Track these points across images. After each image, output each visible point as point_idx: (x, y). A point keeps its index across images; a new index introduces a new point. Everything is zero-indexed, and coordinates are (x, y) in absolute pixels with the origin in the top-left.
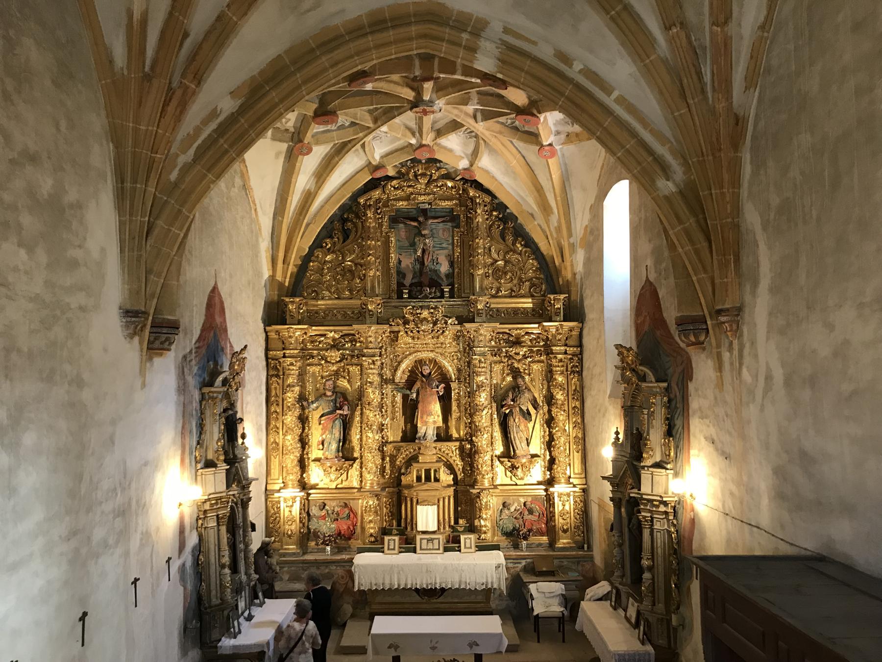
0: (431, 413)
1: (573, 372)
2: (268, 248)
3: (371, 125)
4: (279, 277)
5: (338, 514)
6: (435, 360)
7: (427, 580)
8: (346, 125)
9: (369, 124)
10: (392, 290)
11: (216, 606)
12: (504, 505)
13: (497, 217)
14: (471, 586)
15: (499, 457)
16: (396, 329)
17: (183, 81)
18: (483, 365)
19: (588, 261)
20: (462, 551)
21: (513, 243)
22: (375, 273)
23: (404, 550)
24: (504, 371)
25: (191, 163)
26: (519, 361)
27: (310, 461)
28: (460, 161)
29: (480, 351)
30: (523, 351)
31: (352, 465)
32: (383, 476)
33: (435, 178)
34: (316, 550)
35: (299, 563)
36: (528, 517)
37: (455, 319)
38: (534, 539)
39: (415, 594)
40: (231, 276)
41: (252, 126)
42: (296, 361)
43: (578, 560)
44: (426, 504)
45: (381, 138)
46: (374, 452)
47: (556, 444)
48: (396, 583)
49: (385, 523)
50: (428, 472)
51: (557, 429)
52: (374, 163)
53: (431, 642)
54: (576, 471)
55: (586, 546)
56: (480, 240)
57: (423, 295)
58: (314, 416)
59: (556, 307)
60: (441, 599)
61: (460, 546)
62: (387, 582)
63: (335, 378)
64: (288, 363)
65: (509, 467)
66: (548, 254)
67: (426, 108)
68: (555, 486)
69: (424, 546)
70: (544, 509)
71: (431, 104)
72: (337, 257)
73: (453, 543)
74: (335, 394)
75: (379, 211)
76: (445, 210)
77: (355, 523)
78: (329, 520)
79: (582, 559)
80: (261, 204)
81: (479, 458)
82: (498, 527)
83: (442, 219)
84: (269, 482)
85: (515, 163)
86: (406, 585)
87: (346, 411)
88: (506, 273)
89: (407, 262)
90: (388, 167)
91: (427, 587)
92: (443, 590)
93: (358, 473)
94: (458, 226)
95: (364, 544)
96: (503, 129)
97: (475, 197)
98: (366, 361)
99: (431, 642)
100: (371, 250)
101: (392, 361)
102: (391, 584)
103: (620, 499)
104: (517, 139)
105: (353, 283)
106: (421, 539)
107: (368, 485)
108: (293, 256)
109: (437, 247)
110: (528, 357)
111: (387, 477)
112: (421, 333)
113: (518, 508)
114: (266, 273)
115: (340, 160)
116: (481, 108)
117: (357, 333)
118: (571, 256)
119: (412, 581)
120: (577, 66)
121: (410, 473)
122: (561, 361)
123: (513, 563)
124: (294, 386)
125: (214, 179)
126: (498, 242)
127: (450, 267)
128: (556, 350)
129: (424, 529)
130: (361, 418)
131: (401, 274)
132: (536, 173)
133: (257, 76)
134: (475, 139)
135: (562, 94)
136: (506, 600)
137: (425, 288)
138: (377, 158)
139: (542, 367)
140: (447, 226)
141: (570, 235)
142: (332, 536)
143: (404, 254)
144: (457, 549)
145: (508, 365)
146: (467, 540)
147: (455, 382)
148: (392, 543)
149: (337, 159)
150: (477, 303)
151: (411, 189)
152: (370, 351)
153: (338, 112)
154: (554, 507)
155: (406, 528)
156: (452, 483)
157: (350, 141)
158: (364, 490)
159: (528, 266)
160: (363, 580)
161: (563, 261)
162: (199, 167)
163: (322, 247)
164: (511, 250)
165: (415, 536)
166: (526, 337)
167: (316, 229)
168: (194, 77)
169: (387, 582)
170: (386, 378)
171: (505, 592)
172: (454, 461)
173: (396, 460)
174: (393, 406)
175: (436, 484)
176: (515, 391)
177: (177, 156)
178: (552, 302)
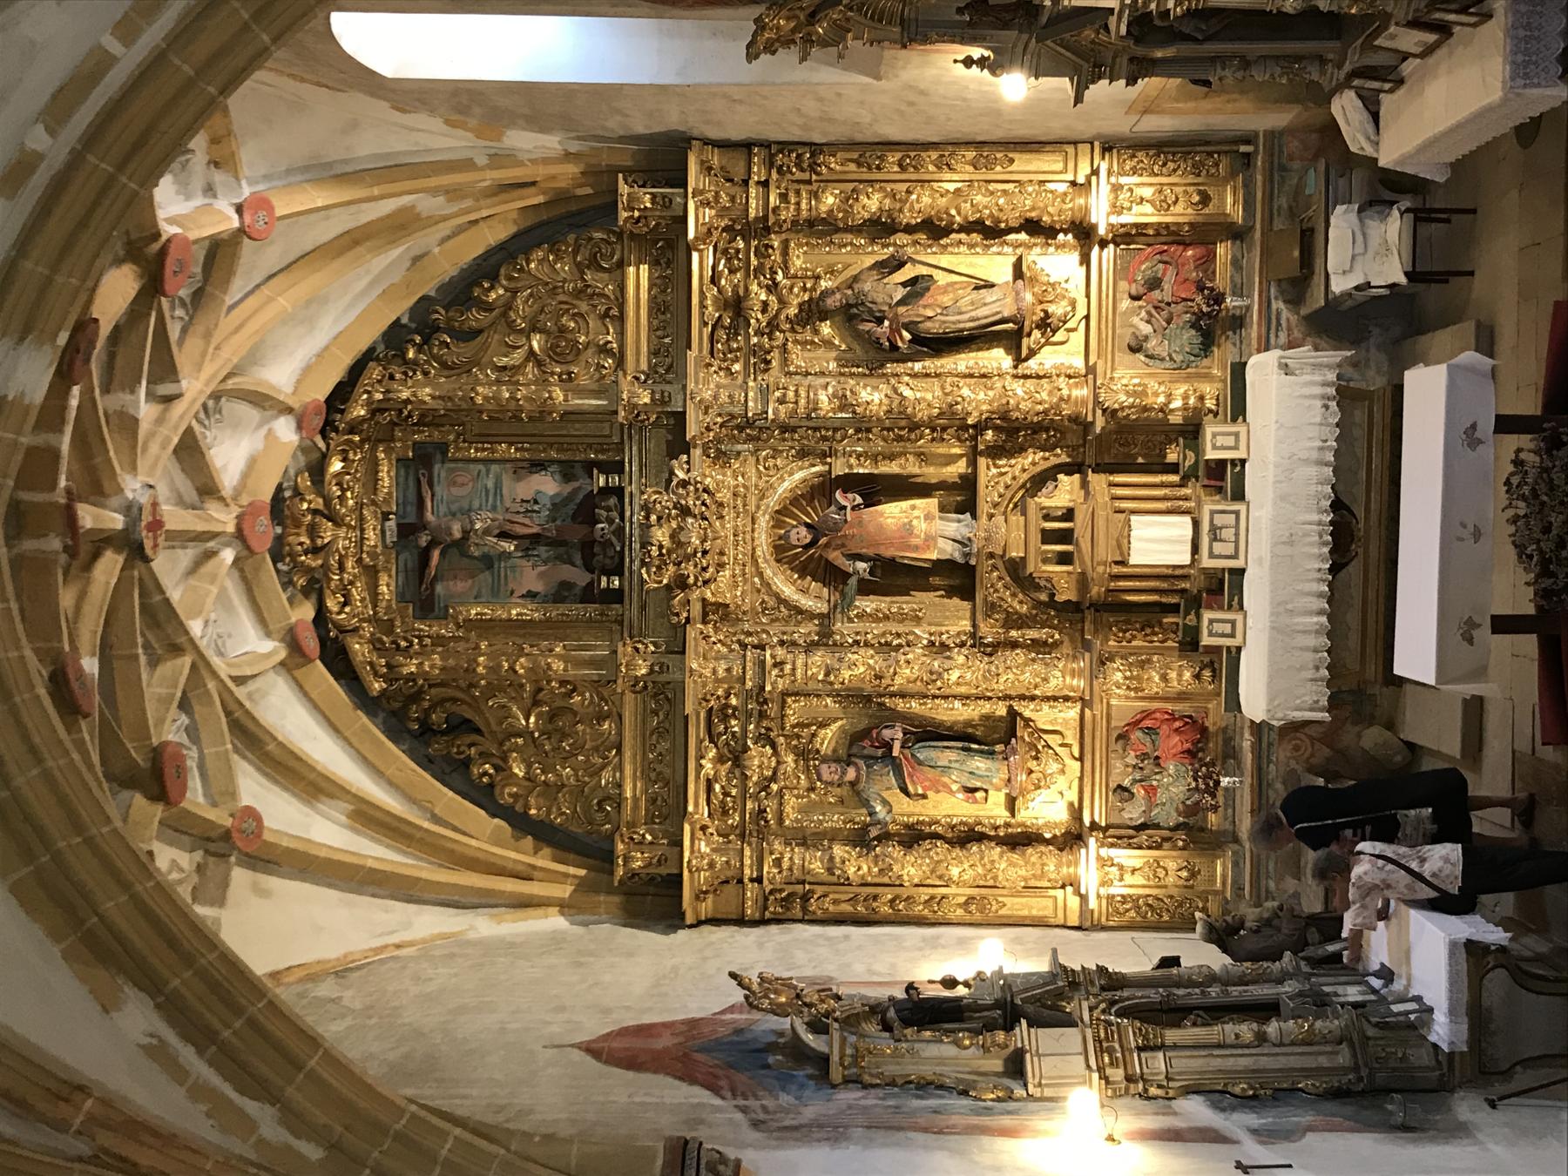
0: (905, 524)
1: (813, 168)
2: (492, 916)
3: (187, 661)
4: (564, 891)
5: (1144, 756)
6: (777, 512)
7: (1311, 544)
8: (187, 721)
9: (183, 666)
10: (601, 615)
11: (1354, 1055)
12: (1134, 349)
13: (420, 350)
15: (1019, 360)
16: (696, 609)
17: (73, 1129)
18: (791, 394)
19: (537, 122)
20: (1244, 456)
21: (486, 310)
22: (559, 657)
23: (1236, 598)
24: (805, 343)
25: (279, 1110)
26: (783, 303)
27: (1013, 821)
29: (756, 401)
30: (759, 294)
31: (1027, 721)
32: (1056, 645)
33: (320, 501)
34: (1230, 811)
37: (674, 462)
38: (1222, 278)
39: (1342, 574)
40: (561, 1009)
41: (188, 960)
42: (771, 853)
43: (1277, 170)
44: (1126, 541)
45: (220, 637)
46: (997, 668)
47: (991, 215)
48: (1315, 619)
49: (1170, 643)
50: (1048, 537)
51: (953, 212)
52: (283, 654)
53: (1462, 540)
54: (1059, 166)
55: (1243, 149)
56: (477, 394)
57: (614, 540)
58: (905, 809)
59: (648, 205)
60: (1360, 512)
61: (1233, 462)
62: (1312, 641)
63: (814, 759)
64: (776, 871)
65: (1043, 334)
66: (515, 222)
67: (143, 524)
68: (1093, 220)
69: (1228, 549)
70: (1149, 250)
71: (135, 510)
72: (516, 748)
73: (1222, 478)
74: (853, 759)
75: (403, 644)
76: (401, 480)
77: (1166, 716)
78: (1158, 777)
79: (1276, 161)
81: (1018, 408)
82: (1188, 367)
83: (425, 487)
84: (1061, 922)
85: (284, 300)
86: (1320, 595)
87: (896, 734)
88: (563, 330)
89: (531, 576)
90: (293, 620)
91: (1325, 544)
92: (1337, 505)
93: (1045, 707)
94: (443, 448)
95: (1219, 694)
96: (199, 328)
97: (369, 402)
98: (776, 682)
99: (1462, 540)
100: (500, 666)
101: (777, 620)
102: (1317, 632)
103: (1131, 60)
104: (225, 293)
105: (581, 711)
106: (1212, 555)
107: (1075, 682)
108: (513, 855)
109: (495, 501)
110: (773, 280)
111: (1057, 636)
112: (707, 546)
113: (1143, 314)
114: (555, 922)
115: (275, 739)
116: (144, 383)
117: (704, 704)
118: (521, 164)
119: (1312, 580)
120: (39, 139)
121: (1049, 580)
122: (784, 197)
123: (1277, 330)
124: (832, 859)
125: (320, 1053)
126: (485, 347)
127: (545, 469)
128: (757, 210)
130: (913, 697)
131: (561, 593)
132: (309, 248)
133: (63, 946)
134: (223, 399)
135: (111, 181)
136: (1368, 351)
137: (598, 534)
138: (270, 647)
139: (800, 245)
140: (443, 474)
141: (467, 165)
142: (1196, 771)
143: (511, 586)
144: (1238, 468)
145: (793, 330)
146: (1218, 444)
147: (830, 464)
148: (1218, 627)
149: (271, 747)
150: (635, 406)
151: (350, 564)
152: (749, 674)
153: (155, 741)
154: (1146, 225)
155: (1183, 591)
156: (1077, 476)
157: (228, 714)
158: (1087, 693)
159: (543, 273)
160: (1306, 698)
161: (533, 184)
162: (290, 1091)
163: (491, 786)
164: (504, 314)
166: (723, 282)
167: (447, 799)
168: (67, 1100)
169: (1312, 641)
170: (818, 634)
171: (1349, 354)
172: (1024, 470)
173: (1017, 613)
174: (887, 618)
175: (1079, 516)
176: (855, 316)
177: (262, 1143)
178: (637, 214)
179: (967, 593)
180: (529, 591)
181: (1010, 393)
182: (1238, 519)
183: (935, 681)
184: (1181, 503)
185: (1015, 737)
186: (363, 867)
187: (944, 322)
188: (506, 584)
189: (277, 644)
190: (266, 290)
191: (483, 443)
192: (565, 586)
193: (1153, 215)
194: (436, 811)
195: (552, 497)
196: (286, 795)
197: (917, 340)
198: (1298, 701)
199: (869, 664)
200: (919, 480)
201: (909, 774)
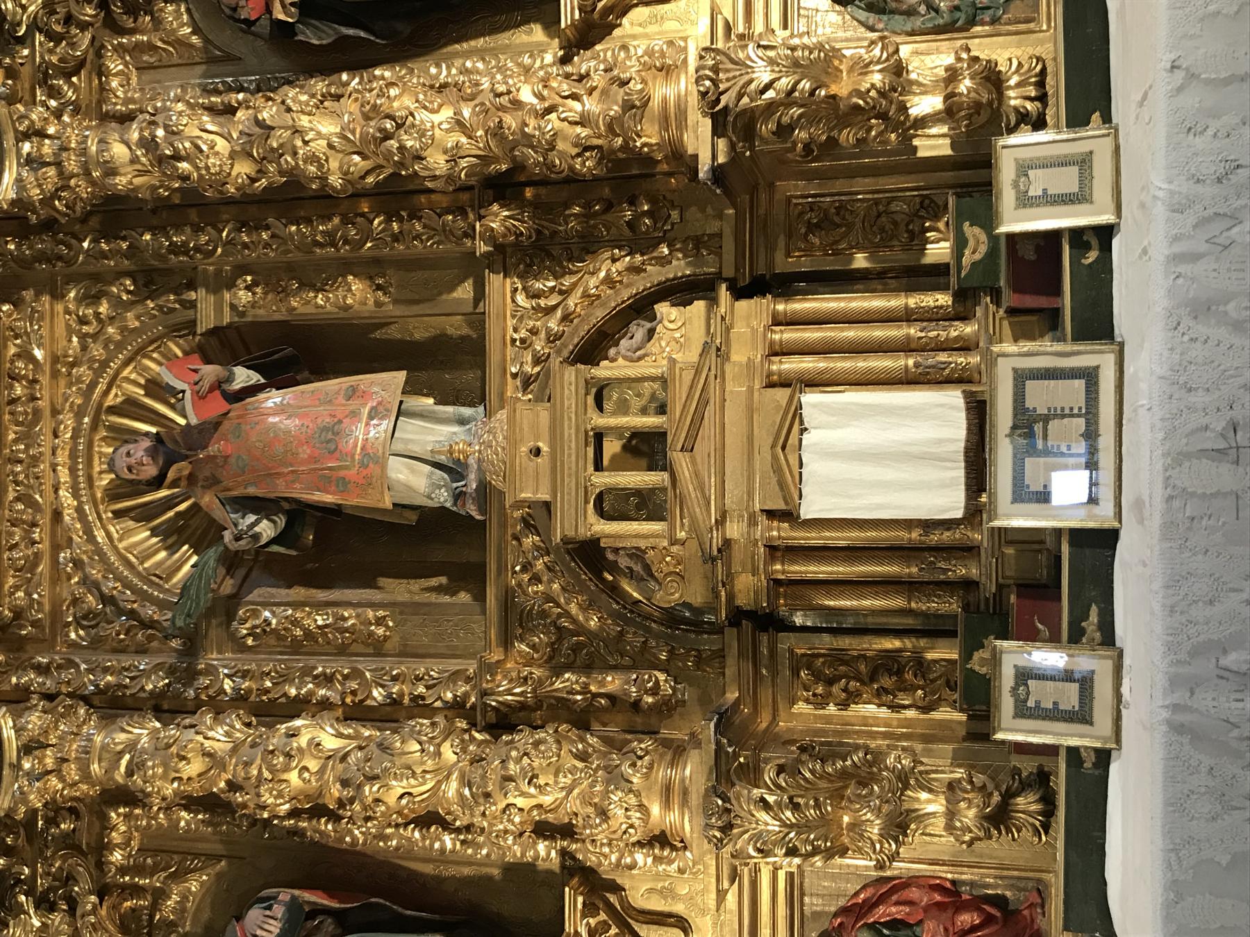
0: (325, 429)
6: (112, 410)
20: (1106, 218)
23: (1094, 616)
24: (139, 48)
61: (1078, 236)
77: (938, 898)
121: (637, 554)
129: (958, 473)
144: (1092, 256)
147: (192, 305)
155: (968, 585)
156: (699, 306)
165: (1005, 536)
170: (171, 671)
173: (581, 630)
181: (504, 100)
183: (352, 801)
184: (943, 357)
200: (394, 333)
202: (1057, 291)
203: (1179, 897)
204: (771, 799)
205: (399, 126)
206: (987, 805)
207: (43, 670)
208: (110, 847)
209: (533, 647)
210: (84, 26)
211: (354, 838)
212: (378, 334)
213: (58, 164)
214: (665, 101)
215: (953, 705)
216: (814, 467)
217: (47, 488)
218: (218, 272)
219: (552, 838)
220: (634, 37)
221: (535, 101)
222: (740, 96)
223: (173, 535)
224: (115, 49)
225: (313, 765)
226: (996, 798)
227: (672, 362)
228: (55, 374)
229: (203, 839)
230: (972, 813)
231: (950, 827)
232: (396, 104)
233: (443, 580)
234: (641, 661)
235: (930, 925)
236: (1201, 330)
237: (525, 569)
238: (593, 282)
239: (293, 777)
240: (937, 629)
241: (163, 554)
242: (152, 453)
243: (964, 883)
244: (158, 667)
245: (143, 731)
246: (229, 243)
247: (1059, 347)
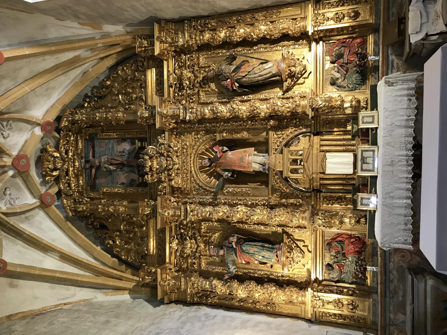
0: (241, 158)
2: (104, 293)
5: (338, 252)
6: (200, 154)
7: (403, 165)
12: (333, 83)
14: (412, 114)
18: (194, 110)
24: (206, 91)
28: (35, 134)
32: (301, 205)
34: (375, 279)
35: (385, 301)
36: (345, 59)
48: (405, 201)
51: (252, 34)
54: (299, 12)
56: (97, 116)
61: (372, 129)
62: (403, 211)
66: (115, 58)
76: (86, 146)
77: (348, 236)
78: (344, 261)
80: (63, 299)
81: (279, 111)
82: (355, 89)
84: (303, 317)
86: (408, 190)
87: (234, 239)
89: (122, 177)
91: (410, 165)
102: (406, 207)
109: (112, 152)
111: (301, 202)
113: (336, 69)
114: (126, 297)
118: (112, 37)
123: (392, 69)
127: (126, 141)
129: (352, 166)
132: (41, 70)
140: (97, 144)
141: (93, 39)
143: (117, 181)
144: (374, 132)
145: (201, 86)
147: (216, 136)
155: (354, 185)
160: (400, 238)
161: (119, 44)
165: (360, 176)
169: (403, 211)
170: (212, 199)
173: (285, 192)
178: (143, 49)
179: (266, 183)
180: (122, 182)
181: (275, 104)
182: (374, 155)
183: (248, 219)
184: (350, 147)
185: (283, 242)
186: (55, 277)
187: (250, 78)
188: (116, 179)
189: (37, 200)
190: (23, 85)
191: (117, 132)
192: (133, 181)
193: (334, 24)
194: (94, 255)
195: (128, 150)
196: (36, 250)
197: (241, 86)
198: (396, 239)
199: (224, 212)
200: (251, 141)
201: (239, 255)
202: (369, 137)
203: (383, 229)
204: (321, 218)
205: (257, 108)
206: (356, 220)
207: (189, 199)
208: (202, 229)
209: (277, 195)
210: (196, 87)
211: (246, 227)
212: (248, 141)
213: (196, 113)
214: (303, 104)
215: (351, 205)
216: (328, 165)
217: (189, 167)
218: (220, 130)
219: (281, 227)
220: (296, 90)
221: (281, 105)
222: (316, 106)
223: (210, 175)
224: (202, 91)
225: (242, 214)
226: (357, 219)
227: (304, 147)
228: (190, 147)
229: (218, 227)
230: (354, 221)
231: (350, 224)
232: (256, 105)
233: (259, 184)
234: (297, 197)
235: (346, 241)
236: (388, 147)
237: (275, 182)
238: (288, 133)
239: (238, 215)
240: (348, 192)
241: (209, 179)
242: (209, 161)
243: (352, 234)
244: (210, 198)
245: (208, 209)
246: (222, 125)
247: (368, 146)
